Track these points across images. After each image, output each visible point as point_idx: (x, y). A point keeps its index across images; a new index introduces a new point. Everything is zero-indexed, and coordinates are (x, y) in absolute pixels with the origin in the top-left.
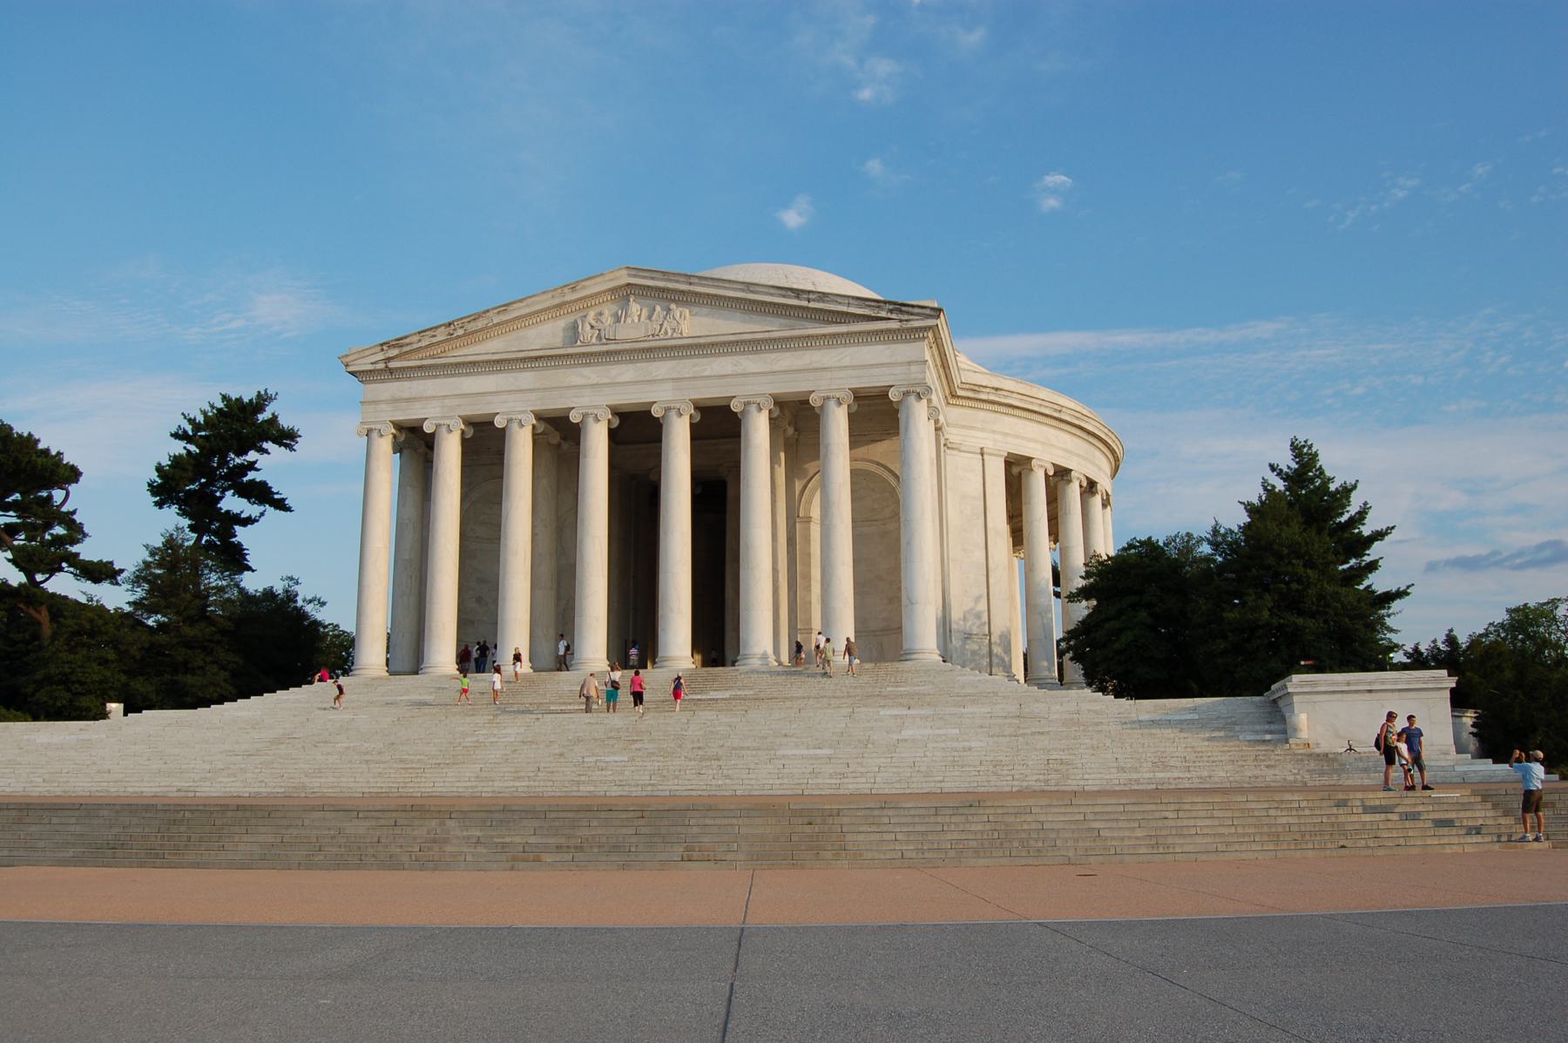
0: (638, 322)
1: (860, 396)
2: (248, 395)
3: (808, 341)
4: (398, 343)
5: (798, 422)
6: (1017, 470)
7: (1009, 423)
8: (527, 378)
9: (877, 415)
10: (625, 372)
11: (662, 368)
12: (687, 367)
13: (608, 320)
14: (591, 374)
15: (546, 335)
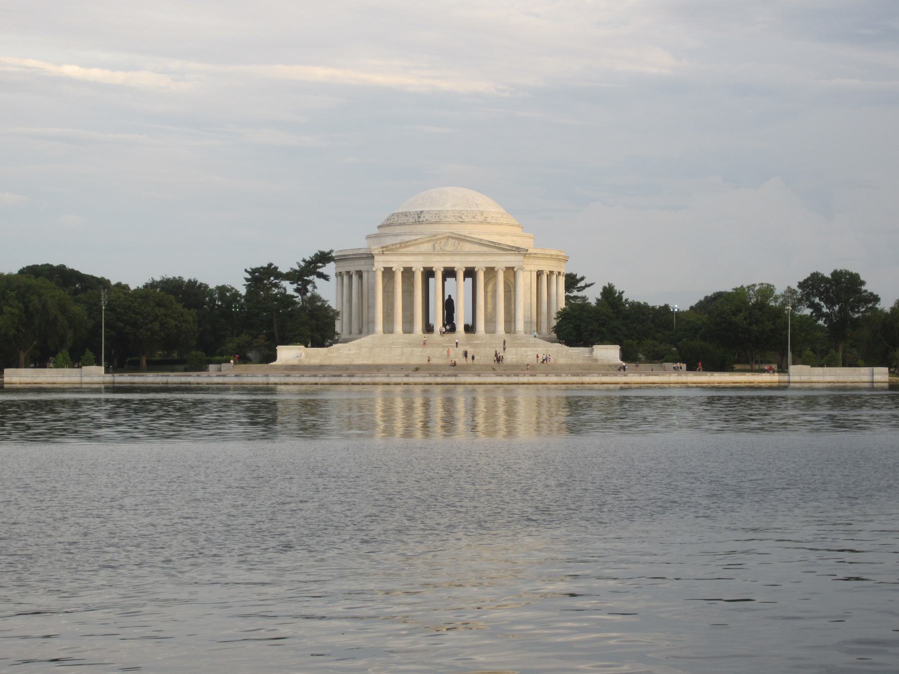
0: (450, 246)
1: (508, 268)
2: (327, 250)
3: (495, 254)
4: (386, 247)
5: (490, 272)
6: (539, 274)
7: (537, 262)
8: (420, 258)
9: (511, 272)
10: (447, 258)
11: (457, 258)
12: (464, 258)
13: (443, 244)
14: (438, 258)
15: (426, 247)
